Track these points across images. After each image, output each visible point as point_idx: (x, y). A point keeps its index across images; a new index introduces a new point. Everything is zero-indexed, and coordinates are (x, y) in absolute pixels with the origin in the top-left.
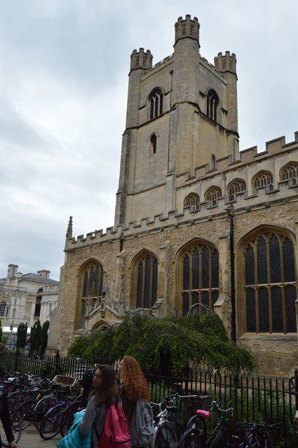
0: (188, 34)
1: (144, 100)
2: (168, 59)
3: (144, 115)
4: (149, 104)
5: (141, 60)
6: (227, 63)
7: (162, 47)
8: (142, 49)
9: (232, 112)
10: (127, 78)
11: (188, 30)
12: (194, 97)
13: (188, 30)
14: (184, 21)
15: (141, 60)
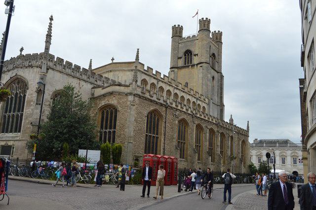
0: (206, 28)
1: (181, 54)
2: (194, 36)
3: (181, 63)
4: (184, 57)
5: (177, 31)
6: (218, 37)
7: (191, 30)
8: (179, 25)
9: (220, 63)
10: (171, 40)
11: (205, 24)
12: (208, 60)
13: (205, 24)
14: (204, 21)
15: (177, 31)
